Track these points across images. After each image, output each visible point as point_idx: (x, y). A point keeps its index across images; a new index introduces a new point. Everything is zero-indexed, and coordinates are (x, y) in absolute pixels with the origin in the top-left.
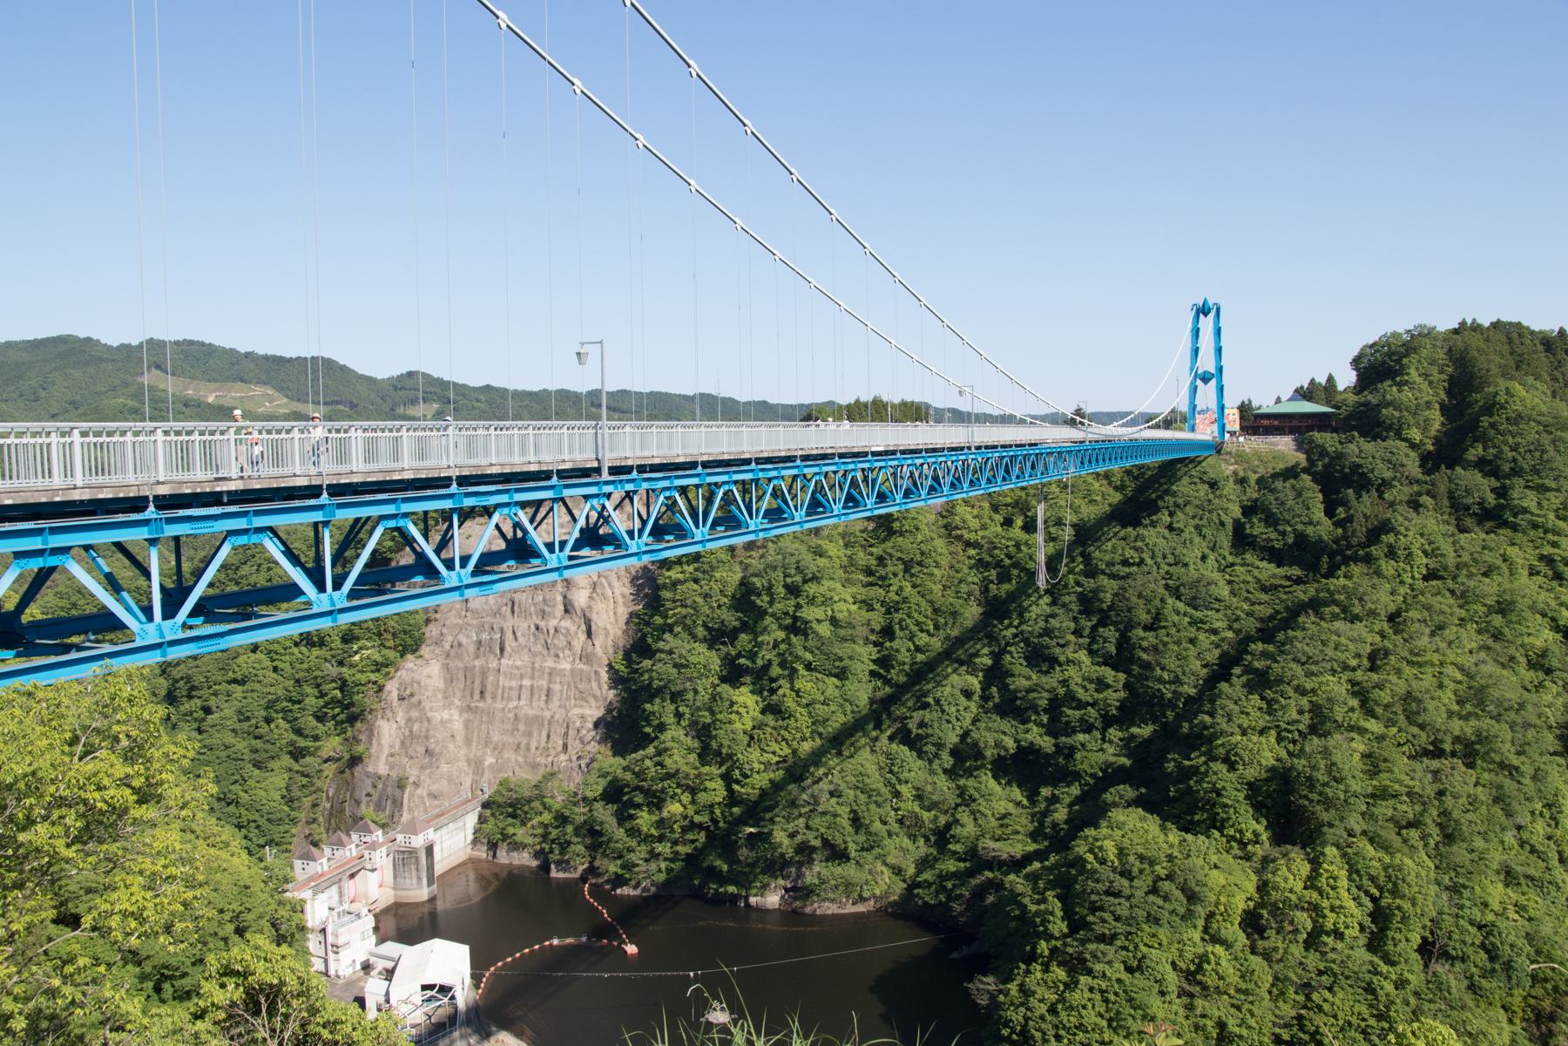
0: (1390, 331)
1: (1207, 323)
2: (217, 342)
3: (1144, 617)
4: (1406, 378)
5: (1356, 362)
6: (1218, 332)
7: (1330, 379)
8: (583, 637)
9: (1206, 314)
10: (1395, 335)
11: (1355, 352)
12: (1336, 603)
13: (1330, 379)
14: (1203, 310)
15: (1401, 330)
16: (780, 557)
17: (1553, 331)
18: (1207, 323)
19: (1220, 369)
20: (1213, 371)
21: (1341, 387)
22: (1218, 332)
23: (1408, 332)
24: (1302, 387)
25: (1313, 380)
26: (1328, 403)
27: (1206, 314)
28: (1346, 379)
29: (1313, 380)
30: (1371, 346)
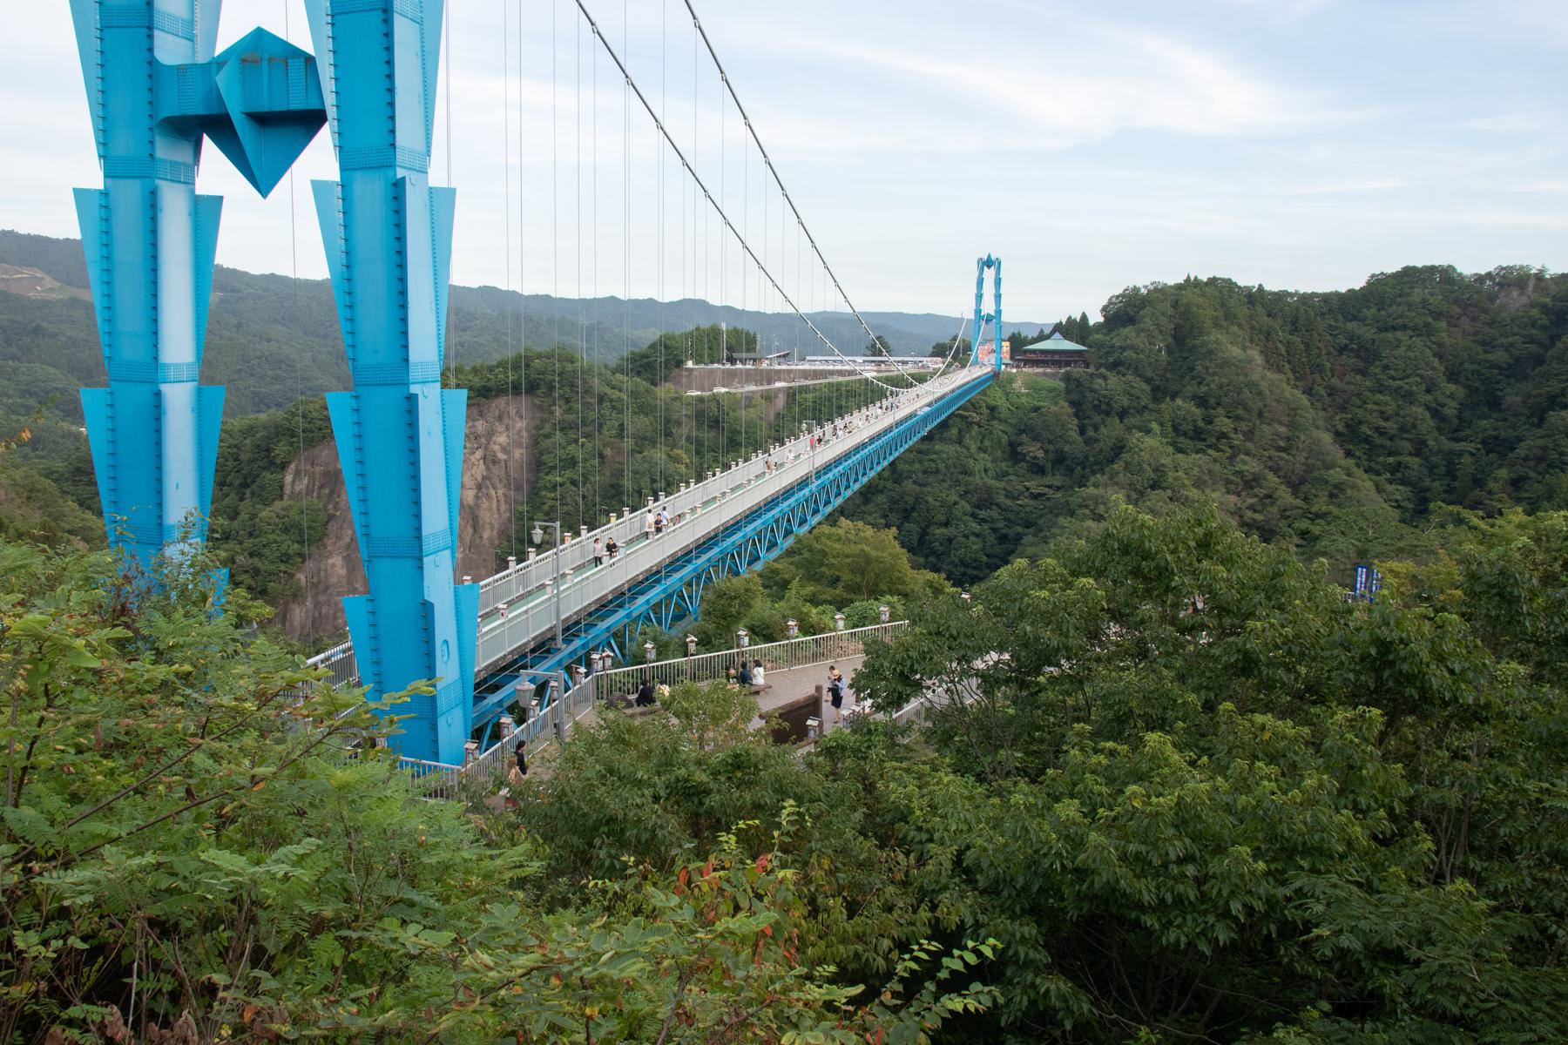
0: (1131, 286)
1: (989, 274)
3: (941, 518)
4: (1142, 325)
5: (1104, 309)
6: (998, 282)
7: (1084, 317)
8: (470, 531)
9: (989, 267)
10: (1136, 289)
11: (1105, 302)
12: (1086, 507)
13: (1084, 317)
14: (988, 263)
15: (1139, 284)
16: (645, 465)
19: (999, 312)
21: (1091, 323)
22: (998, 282)
23: (1145, 287)
26: (1081, 341)
27: (989, 267)
28: (1095, 318)
30: (1117, 297)
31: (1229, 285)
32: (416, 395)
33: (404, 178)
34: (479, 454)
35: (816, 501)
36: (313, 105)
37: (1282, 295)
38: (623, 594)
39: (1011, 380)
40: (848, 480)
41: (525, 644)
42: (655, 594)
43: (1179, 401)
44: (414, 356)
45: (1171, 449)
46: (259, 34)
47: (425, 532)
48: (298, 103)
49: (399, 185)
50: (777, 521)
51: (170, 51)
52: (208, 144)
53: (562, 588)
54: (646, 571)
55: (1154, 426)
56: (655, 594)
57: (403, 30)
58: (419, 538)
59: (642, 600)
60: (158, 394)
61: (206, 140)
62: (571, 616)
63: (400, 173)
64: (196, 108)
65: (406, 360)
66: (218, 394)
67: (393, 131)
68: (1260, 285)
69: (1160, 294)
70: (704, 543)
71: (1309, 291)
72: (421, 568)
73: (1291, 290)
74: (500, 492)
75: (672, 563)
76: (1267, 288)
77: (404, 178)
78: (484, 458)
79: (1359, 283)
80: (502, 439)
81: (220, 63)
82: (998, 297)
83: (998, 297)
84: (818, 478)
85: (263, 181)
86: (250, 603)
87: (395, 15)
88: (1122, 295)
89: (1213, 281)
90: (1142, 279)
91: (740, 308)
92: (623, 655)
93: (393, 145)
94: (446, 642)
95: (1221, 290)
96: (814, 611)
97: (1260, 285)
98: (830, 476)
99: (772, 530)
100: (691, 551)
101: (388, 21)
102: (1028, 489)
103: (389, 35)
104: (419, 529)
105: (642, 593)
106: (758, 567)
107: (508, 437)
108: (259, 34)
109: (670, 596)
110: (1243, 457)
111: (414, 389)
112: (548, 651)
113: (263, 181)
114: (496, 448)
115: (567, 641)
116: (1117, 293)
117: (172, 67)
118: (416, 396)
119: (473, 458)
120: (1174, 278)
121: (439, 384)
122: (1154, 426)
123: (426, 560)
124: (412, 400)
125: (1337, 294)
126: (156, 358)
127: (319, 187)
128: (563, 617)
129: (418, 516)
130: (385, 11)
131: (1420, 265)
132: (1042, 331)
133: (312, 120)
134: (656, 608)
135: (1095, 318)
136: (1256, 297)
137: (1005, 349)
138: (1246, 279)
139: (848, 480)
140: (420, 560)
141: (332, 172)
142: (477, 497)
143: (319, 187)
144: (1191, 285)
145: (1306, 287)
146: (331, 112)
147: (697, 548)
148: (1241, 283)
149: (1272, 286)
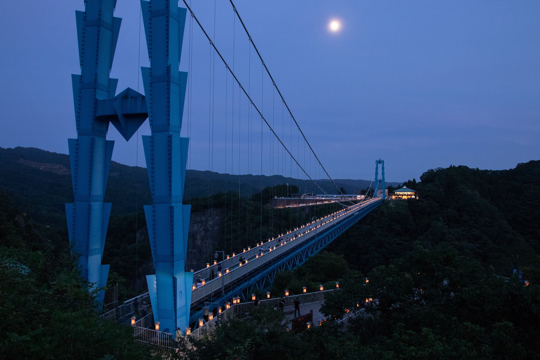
0: (430, 169)
1: (380, 166)
2: (42, 149)
5: (421, 177)
6: (383, 168)
7: (414, 180)
9: (380, 163)
10: (432, 170)
11: (421, 175)
13: (414, 180)
14: (380, 162)
15: (433, 168)
17: (475, 169)
18: (380, 166)
19: (384, 179)
20: (382, 179)
21: (417, 182)
22: (383, 168)
23: (436, 169)
24: (406, 182)
25: (409, 180)
27: (380, 163)
28: (418, 180)
29: (409, 180)
30: (426, 173)
31: (466, 168)
32: (173, 207)
33: (172, 135)
34: (202, 228)
35: (317, 245)
36: (144, 112)
37: (486, 171)
38: (246, 277)
39: (389, 202)
40: (329, 238)
41: (211, 294)
42: (258, 277)
43: (450, 210)
44: (173, 193)
45: (447, 227)
46: (129, 88)
47: (175, 253)
48: (139, 111)
49: (170, 137)
50: (303, 252)
51: (101, 96)
52: (111, 124)
53: (224, 274)
54: (255, 269)
55: (441, 218)
56: (258, 277)
57: (174, 88)
58: (173, 255)
59: (253, 279)
60: (90, 205)
61: (110, 123)
62: (227, 284)
63: (171, 133)
64: (108, 112)
65: (171, 195)
66: (109, 205)
67: (169, 120)
68: (477, 168)
69: (441, 172)
70: (276, 259)
71: (495, 170)
72: (173, 265)
73: (489, 169)
74: (209, 241)
75: (264, 266)
76: (480, 169)
77: (172, 135)
78: (204, 229)
79: (514, 167)
80: (211, 223)
81: (116, 99)
82: (383, 174)
83: (383, 174)
84: (318, 237)
85: (127, 137)
86: (118, 277)
87: (171, 83)
88: (428, 172)
89: (460, 167)
90: (434, 167)
91: (238, 174)
92: (246, 299)
93: (169, 124)
94: (181, 292)
95: (463, 170)
96: (313, 284)
97: (477, 168)
98: (322, 236)
99: (301, 255)
100: (271, 263)
101: (168, 85)
102: (396, 241)
103: (169, 89)
104: (173, 252)
105: (253, 277)
106: (295, 268)
107: (213, 222)
108: (129, 89)
109: (264, 277)
110: (474, 229)
111: (173, 204)
112: (219, 296)
113: (127, 137)
114: (209, 226)
115: (226, 293)
116: (425, 172)
117: (101, 100)
118: (173, 207)
119: (200, 229)
120: (446, 166)
121: (182, 203)
122: (441, 218)
123: (175, 263)
124: (172, 208)
125: (506, 171)
126: (90, 193)
127: (144, 137)
128: (225, 285)
129: (173, 248)
130: (168, 82)
131: (536, 160)
132: (399, 185)
133: (142, 117)
134: (258, 282)
135: (418, 180)
136: (476, 172)
137: (386, 192)
138: (472, 166)
139: (329, 238)
140: (173, 263)
141: (149, 133)
142: (201, 243)
143: (144, 137)
144: (452, 168)
145: (494, 169)
146: (149, 114)
147: (273, 261)
148: (470, 168)
149: (482, 168)
